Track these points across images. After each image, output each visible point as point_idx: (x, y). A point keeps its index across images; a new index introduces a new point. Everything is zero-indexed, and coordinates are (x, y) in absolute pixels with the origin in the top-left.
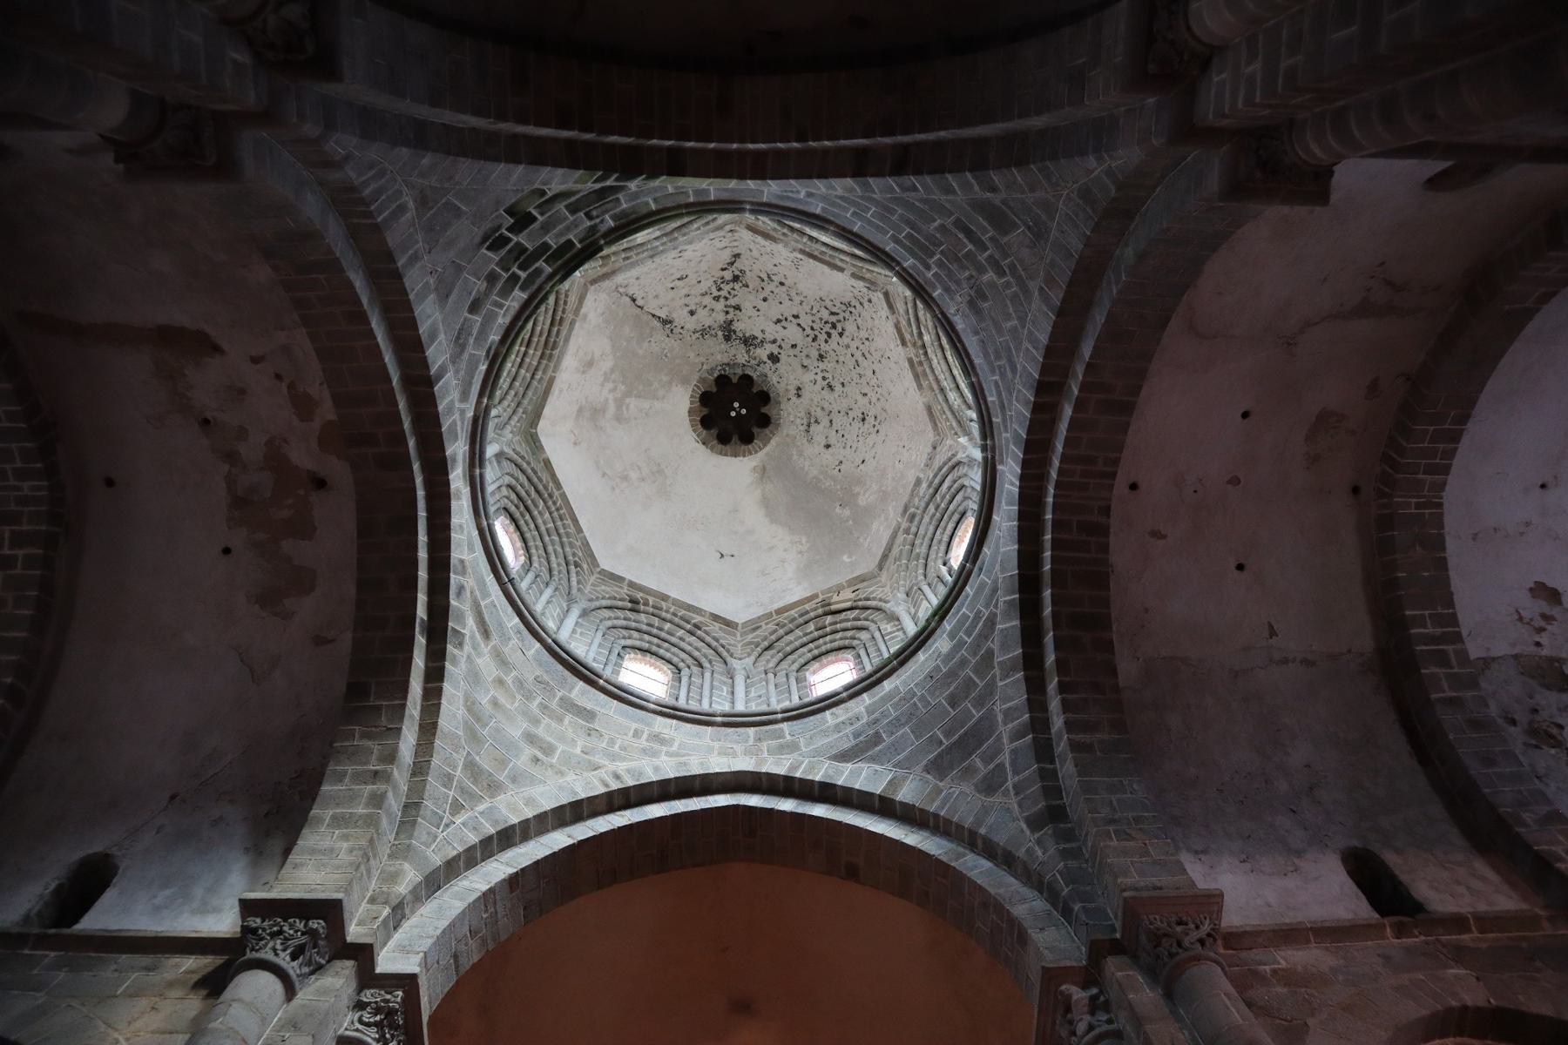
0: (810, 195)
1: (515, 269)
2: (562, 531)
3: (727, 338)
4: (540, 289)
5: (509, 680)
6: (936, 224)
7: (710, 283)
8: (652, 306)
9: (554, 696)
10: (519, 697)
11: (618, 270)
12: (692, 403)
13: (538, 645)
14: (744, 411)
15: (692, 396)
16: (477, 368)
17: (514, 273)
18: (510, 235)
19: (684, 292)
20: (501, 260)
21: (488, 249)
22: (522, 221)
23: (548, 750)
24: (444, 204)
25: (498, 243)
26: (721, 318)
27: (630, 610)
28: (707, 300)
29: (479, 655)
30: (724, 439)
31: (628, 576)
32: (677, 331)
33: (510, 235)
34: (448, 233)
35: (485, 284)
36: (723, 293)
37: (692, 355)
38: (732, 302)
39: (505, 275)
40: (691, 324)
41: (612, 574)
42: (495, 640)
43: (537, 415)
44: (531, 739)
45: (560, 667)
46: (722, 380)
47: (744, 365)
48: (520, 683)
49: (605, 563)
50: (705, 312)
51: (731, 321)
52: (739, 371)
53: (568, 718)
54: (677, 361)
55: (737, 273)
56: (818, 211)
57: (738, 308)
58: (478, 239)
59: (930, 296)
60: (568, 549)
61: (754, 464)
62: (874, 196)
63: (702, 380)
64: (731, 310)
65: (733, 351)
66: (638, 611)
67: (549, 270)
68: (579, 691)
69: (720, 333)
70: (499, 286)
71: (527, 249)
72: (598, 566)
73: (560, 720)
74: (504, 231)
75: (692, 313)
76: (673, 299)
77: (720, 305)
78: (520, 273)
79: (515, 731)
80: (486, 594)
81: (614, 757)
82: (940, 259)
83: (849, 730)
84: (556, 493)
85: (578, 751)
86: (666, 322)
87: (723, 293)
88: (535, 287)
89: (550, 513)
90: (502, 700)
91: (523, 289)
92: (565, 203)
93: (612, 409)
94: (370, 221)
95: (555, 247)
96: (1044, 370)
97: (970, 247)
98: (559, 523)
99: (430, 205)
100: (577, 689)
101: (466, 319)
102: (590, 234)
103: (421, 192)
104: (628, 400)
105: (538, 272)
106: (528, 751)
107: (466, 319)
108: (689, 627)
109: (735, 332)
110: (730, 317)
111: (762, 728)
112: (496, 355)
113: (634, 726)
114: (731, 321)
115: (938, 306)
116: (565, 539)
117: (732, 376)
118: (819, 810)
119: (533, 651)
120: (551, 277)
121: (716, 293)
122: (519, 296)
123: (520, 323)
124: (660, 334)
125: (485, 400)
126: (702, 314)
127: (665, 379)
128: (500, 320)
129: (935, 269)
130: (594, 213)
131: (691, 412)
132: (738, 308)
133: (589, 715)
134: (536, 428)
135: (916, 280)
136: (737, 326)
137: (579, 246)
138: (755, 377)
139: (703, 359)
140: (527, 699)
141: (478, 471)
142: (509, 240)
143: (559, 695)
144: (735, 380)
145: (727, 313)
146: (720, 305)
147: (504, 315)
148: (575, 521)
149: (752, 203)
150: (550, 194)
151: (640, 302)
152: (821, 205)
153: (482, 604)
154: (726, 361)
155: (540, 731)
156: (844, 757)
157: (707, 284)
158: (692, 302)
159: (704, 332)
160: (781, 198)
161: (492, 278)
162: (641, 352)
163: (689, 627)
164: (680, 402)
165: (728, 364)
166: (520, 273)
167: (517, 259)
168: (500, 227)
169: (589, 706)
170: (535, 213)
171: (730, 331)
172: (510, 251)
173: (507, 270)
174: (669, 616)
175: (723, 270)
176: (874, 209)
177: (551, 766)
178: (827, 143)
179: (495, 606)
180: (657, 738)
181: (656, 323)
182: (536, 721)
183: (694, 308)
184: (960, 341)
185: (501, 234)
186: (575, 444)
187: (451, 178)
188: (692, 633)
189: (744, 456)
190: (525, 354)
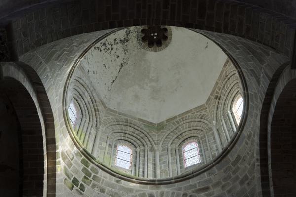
1: (91, 179)
2: (190, 120)
3: (127, 41)
5: (224, 183)
7: (106, 54)
8: (116, 73)
9: (231, 167)
10: (229, 181)
11: (101, 101)
12: (152, 51)
13: (214, 168)
14: (152, 35)
15: (150, 51)
16: (123, 187)
18: (80, 185)
19: (110, 63)
20: (88, 185)
21: (84, 191)
22: (75, 181)
23: (246, 178)
25: (82, 188)
26: (120, 45)
27: (219, 100)
28: (113, 52)
29: (213, 193)
30: (166, 38)
31: (209, 95)
32: (125, 61)
33: (80, 185)
35: (96, 188)
36: (110, 47)
37: (134, 53)
38: (113, 43)
39: (93, 181)
40: (122, 56)
41: (207, 101)
42: (210, 185)
43: (150, 125)
44: (242, 183)
45: (223, 161)
46: (144, 39)
47: (138, 33)
48: (225, 179)
49: (202, 101)
50: (117, 52)
51: (120, 40)
52: (140, 34)
53: (238, 165)
54: (137, 59)
55: (102, 45)
57: (115, 40)
60: (196, 120)
61: (175, 29)
63: (143, 48)
64: (116, 42)
65: (132, 37)
66: (220, 97)
67: (92, 165)
68: (231, 157)
69: (126, 44)
70: (96, 183)
72: (204, 105)
73: (238, 168)
75: (118, 57)
76: (113, 66)
77: (115, 47)
78: (92, 176)
79: (239, 188)
80: (195, 186)
81: (252, 156)
83: (250, 77)
84: (177, 119)
85: (248, 167)
86: (122, 66)
87: (110, 47)
88: (97, 168)
89: (184, 123)
90: (229, 188)
91: (97, 173)
92: (68, 169)
93: (153, 84)
98: (187, 121)
100: (230, 157)
101: (107, 193)
104: (151, 77)
105: (92, 169)
106: (245, 185)
107: (107, 193)
108: (227, 79)
109: (124, 39)
110: (119, 42)
111: (250, 98)
112: (119, 178)
113: (244, 143)
114: (120, 40)
116: (193, 120)
117: (142, 37)
118: (275, 100)
119: (216, 171)
121: (110, 50)
122: (101, 174)
124: (126, 67)
125: (133, 180)
126: (118, 53)
127: (143, 62)
128: (108, 180)
130: (71, 157)
131: (156, 51)
132: (115, 40)
133: (239, 157)
134: (155, 124)
136: (122, 39)
138: (142, 28)
139: (136, 48)
140: (230, 178)
141: (157, 182)
142: (82, 185)
143: (231, 165)
144: (143, 35)
145: (117, 43)
146: (115, 47)
147: (106, 178)
148: (188, 112)
150: (66, 177)
151: (114, 79)
153: (198, 188)
154: (136, 39)
155: (241, 177)
156: (259, 84)
157: (107, 55)
158: (113, 57)
159: (125, 50)
161: (94, 186)
162: (133, 74)
163: (227, 79)
164: (152, 56)
165: (137, 38)
166: (92, 176)
167: (87, 179)
168: (77, 190)
169: (236, 156)
170: (72, 179)
171: (124, 40)
172: (85, 182)
174: (223, 85)
175: (101, 50)
177: (251, 179)
179: (200, 182)
180: (249, 137)
181: (122, 70)
182: (237, 178)
183: (116, 57)
185: (80, 188)
186: (164, 101)
188: (229, 79)
189: (172, 32)
190: (129, 134)
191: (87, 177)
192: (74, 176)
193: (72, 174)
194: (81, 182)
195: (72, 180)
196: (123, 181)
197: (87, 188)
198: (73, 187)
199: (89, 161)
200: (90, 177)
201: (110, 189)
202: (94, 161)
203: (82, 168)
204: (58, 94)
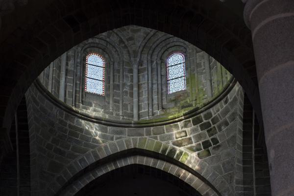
0: (112, 139)
1: (212, 126)
4: (206, 110)
6: (71, 148)
17: (213, 124)
24: (226, 172)
25: (215, 141)
34: (228, 159)
39: (215, 125)
56: (109, 128)
58: (221, 149)
59: (64, 110)
62: (92, 150)
70: (218, 123)
71: (207, 131)
74: (213, 146)
78: (211, 122)
82: (66, 133)
94: (246, 186)
95: (198, 125)
96: (27, 135)
97: (58, 147)
99: (230, 175)
102: (187, 123)
103: (231, 183)
115: (62, 109)
120: (202, 112)
123: (214, 101)
129: (67, 127)
130: (183, 134)
135: (71, 114)
137: (191, 119)
149: (131, 127)
152: (108, 134)
160: (121, 133)
167: (211, 129)
168: (214, 148)
173: (214, 127)
176: (91, 143)
178: (110, 169)
184: (52, 102)
187: (222, 182)
191: (209, 129)
192: (201, 142)
193: (198, 143)
194: (209, 138)
195: (203, 148)
196: (229, 96)
197: (217, 136)
198: (208, 151)
199: (198, 116)
200: (210, 126)
201: (228, 115)
202: (199, 111)
203: (199, 128)
204: (111, 135)
